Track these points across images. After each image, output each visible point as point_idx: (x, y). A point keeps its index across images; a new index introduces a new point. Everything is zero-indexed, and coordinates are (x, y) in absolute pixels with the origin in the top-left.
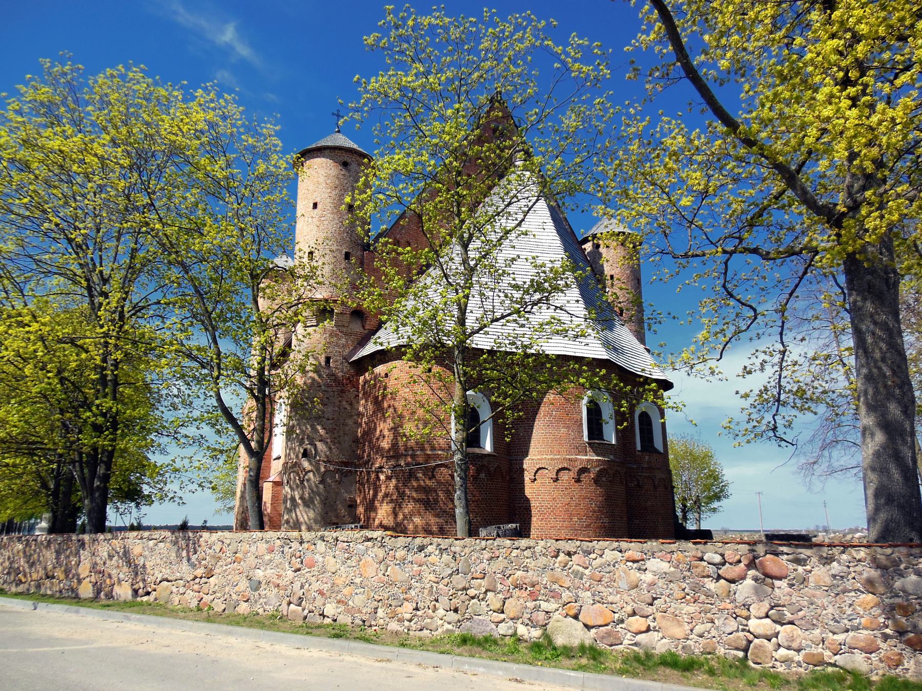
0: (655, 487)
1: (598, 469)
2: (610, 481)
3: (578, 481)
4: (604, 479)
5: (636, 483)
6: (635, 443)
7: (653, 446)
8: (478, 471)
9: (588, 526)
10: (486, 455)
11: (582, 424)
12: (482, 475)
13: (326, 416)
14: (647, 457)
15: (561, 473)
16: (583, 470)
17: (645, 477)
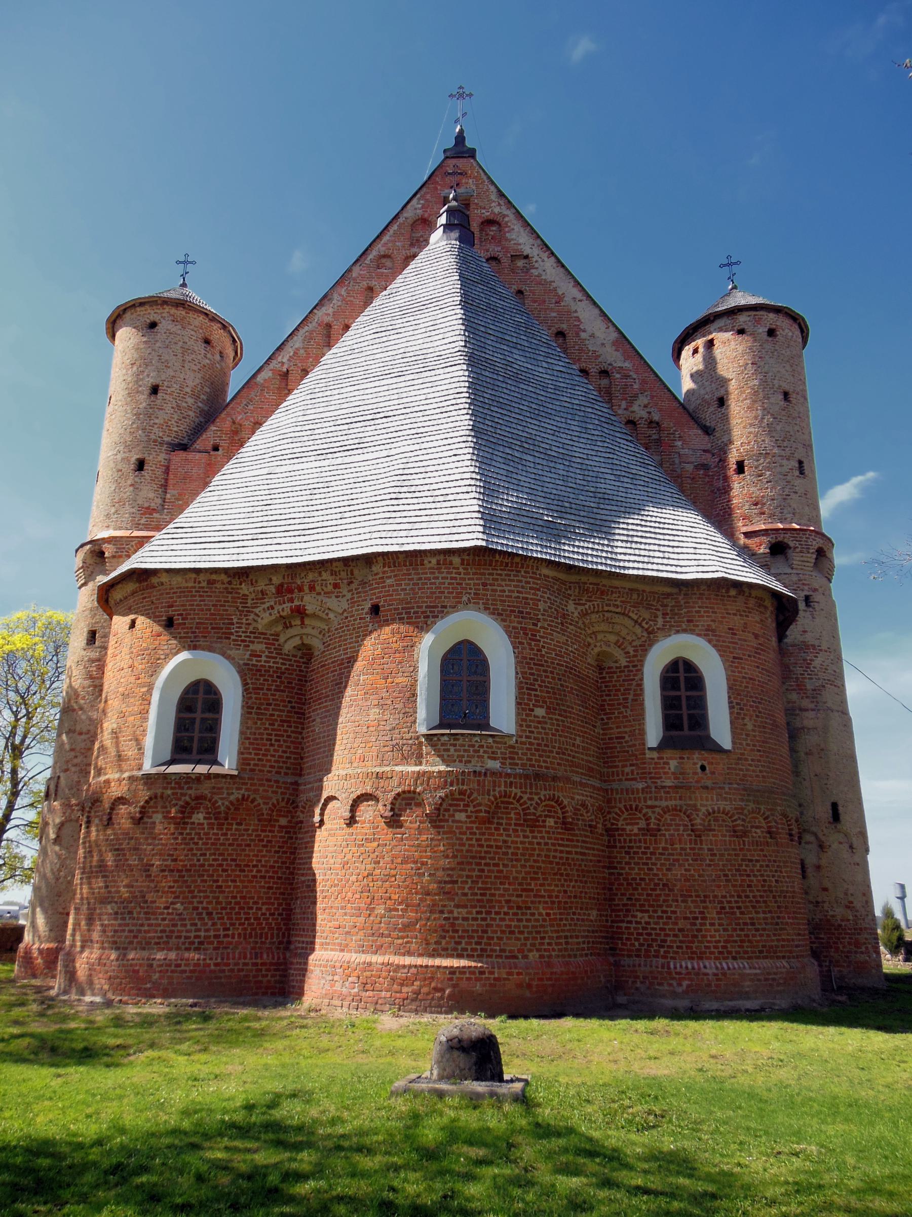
0: (697, 834)
1: (442, 793)
2: (483, 821)
3: (394, 821)
4: (462, 816)
5: (642, 824)
6: (642, 732)
7: (708, 737)
8: (187, 810)
9: (406, 927)
10: (225, 776)
11: (414, 695)
12: (199, 817)
13: (78, 729)
14: (673, 764)
15: (363, 807)
16: (405, 801)
17: (666, 810)
